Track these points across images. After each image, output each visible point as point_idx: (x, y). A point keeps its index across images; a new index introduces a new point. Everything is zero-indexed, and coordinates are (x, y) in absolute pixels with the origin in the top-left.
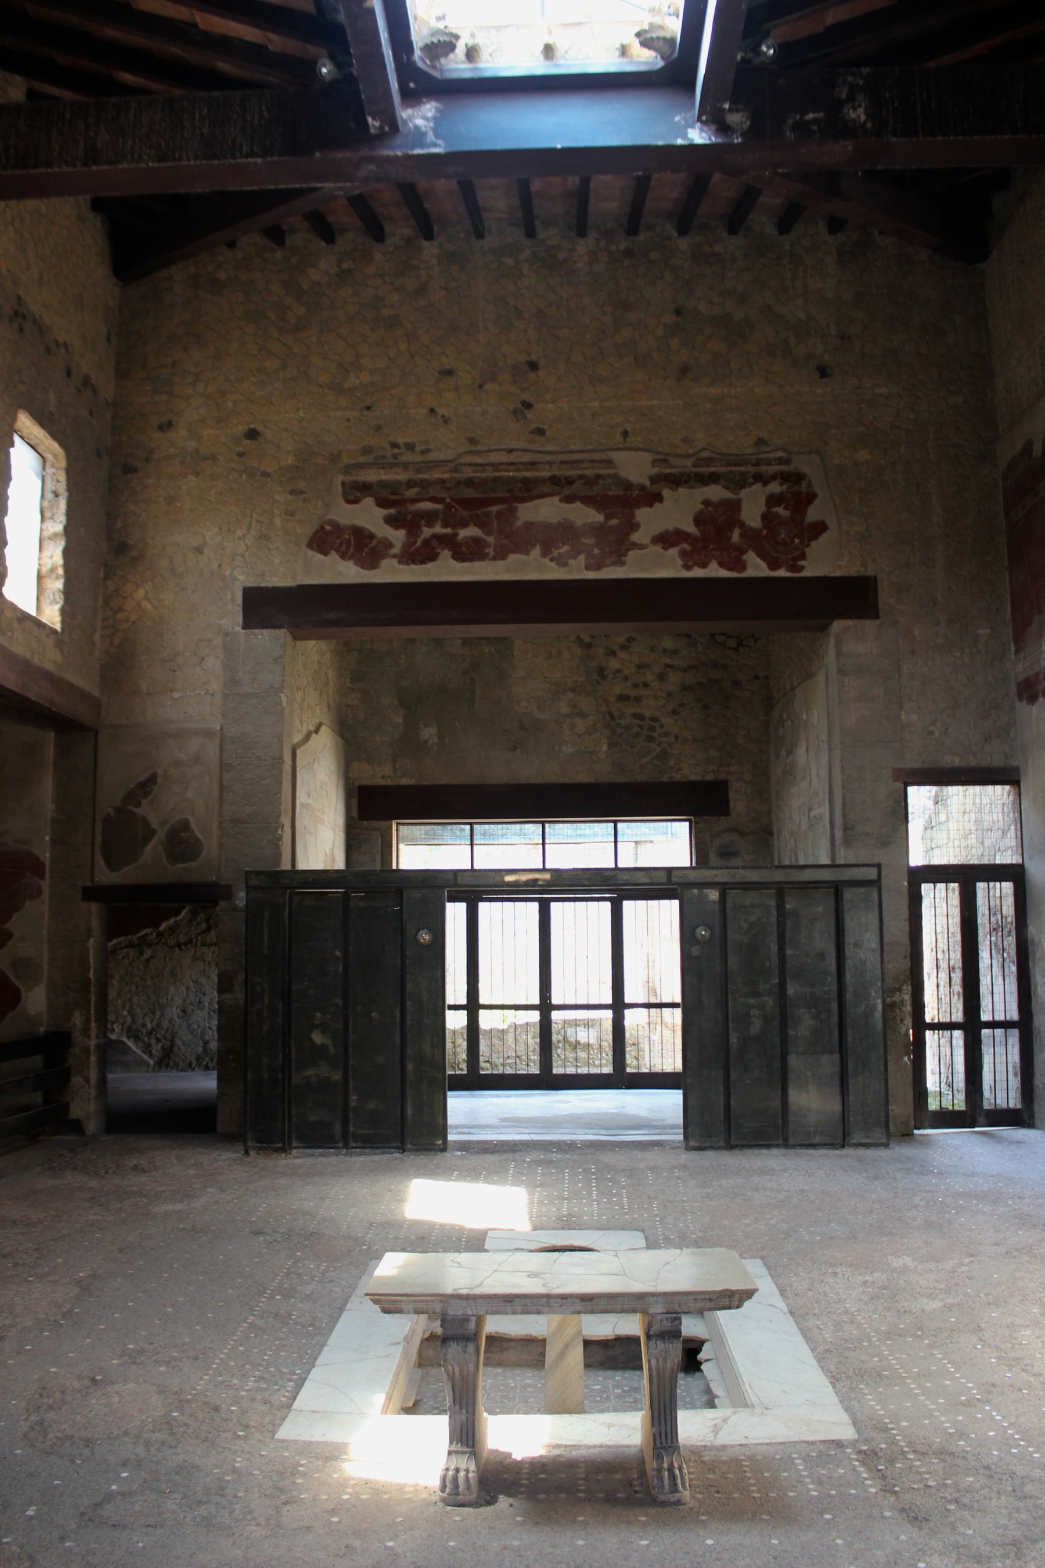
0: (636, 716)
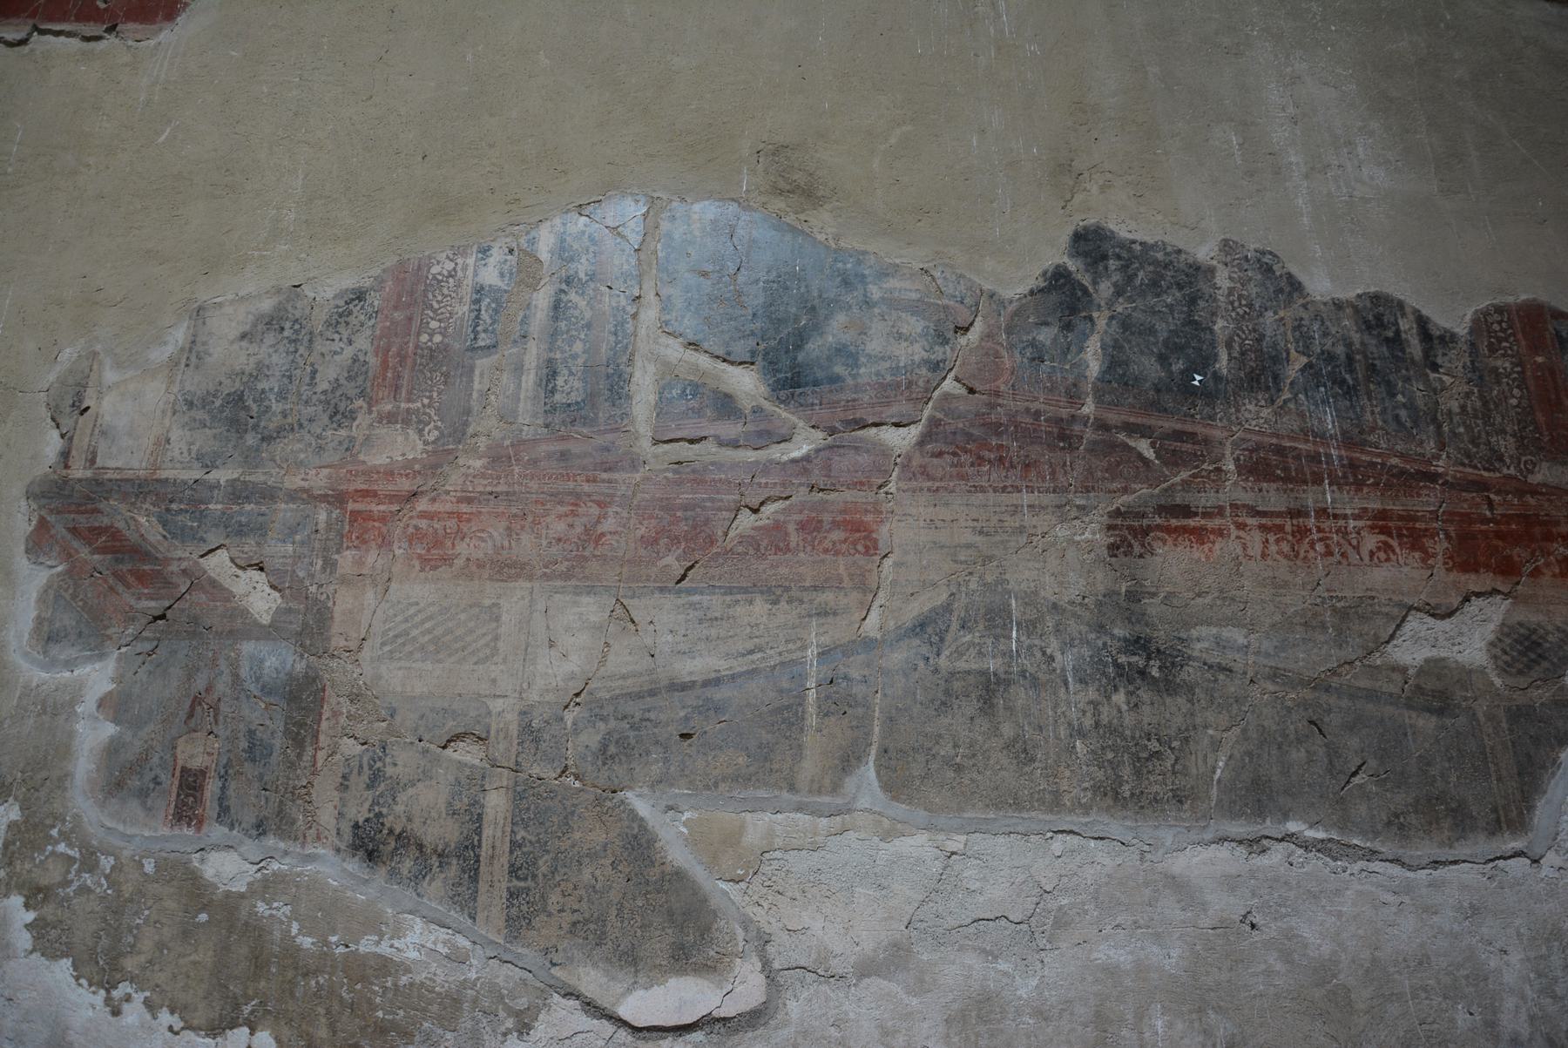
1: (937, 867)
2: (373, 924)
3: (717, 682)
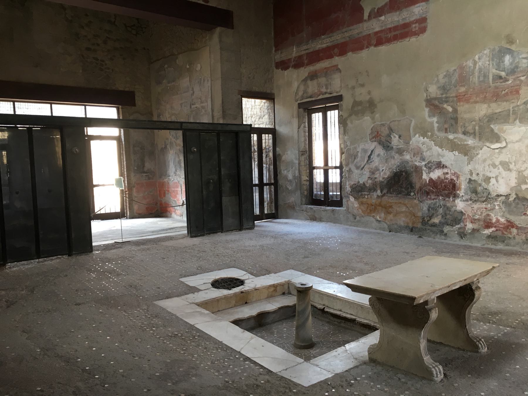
0: (94, 58)
1: (525, 130)
2: (466, 140)
3: (500, 112)
